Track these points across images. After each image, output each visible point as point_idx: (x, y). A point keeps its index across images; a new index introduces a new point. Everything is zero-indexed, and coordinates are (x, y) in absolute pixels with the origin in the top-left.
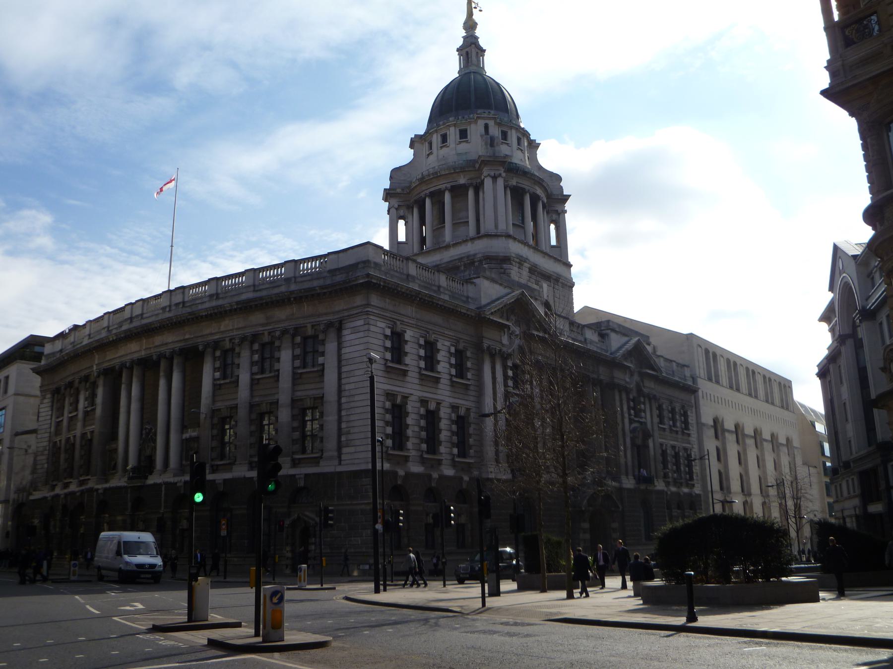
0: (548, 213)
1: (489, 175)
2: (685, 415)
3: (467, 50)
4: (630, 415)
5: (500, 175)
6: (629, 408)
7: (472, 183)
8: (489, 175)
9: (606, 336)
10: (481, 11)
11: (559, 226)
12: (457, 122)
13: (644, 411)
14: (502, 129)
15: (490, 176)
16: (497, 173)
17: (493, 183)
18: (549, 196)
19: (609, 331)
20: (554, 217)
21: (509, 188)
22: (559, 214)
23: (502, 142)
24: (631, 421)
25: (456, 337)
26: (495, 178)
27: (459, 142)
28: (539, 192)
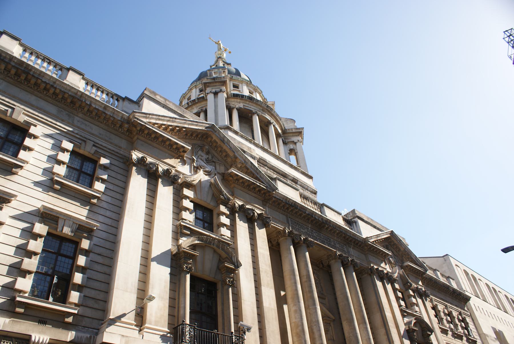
0: (285, 143)
1: (211, 92)
2: (464, 320)
3: (216, 65)
4: (400, 306)
5: (221, 91)
6: (397, 298)
7: (201, 110)
8: (211, 92)
9: (354, 224)
10: (230, 52)
11: (297, 152)
12: (196, 84)
13: (417, 305)
14: (234, 83)
15: (212, 93)
16: (218, 90)
17: (215, 98)
18: (284, 131)
19: (356, 219)
20: (292, 146)
21: (237, 109)
22: (295, 143)
23: (233, 89)
24: (404, 314)
25: (81, 136)
26: (216, 94)
27: (198, 95)
28: (268, 117)
